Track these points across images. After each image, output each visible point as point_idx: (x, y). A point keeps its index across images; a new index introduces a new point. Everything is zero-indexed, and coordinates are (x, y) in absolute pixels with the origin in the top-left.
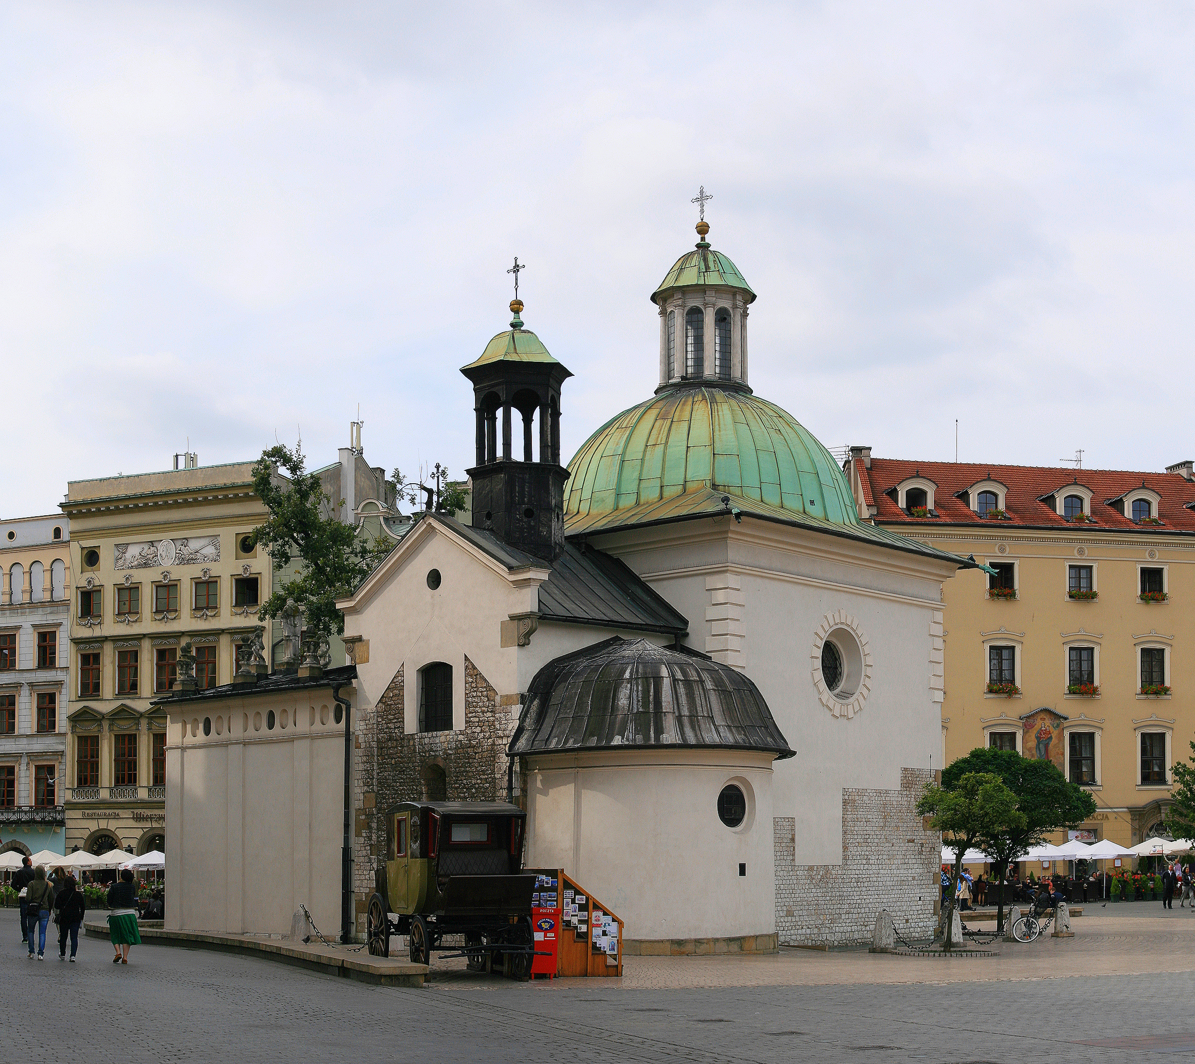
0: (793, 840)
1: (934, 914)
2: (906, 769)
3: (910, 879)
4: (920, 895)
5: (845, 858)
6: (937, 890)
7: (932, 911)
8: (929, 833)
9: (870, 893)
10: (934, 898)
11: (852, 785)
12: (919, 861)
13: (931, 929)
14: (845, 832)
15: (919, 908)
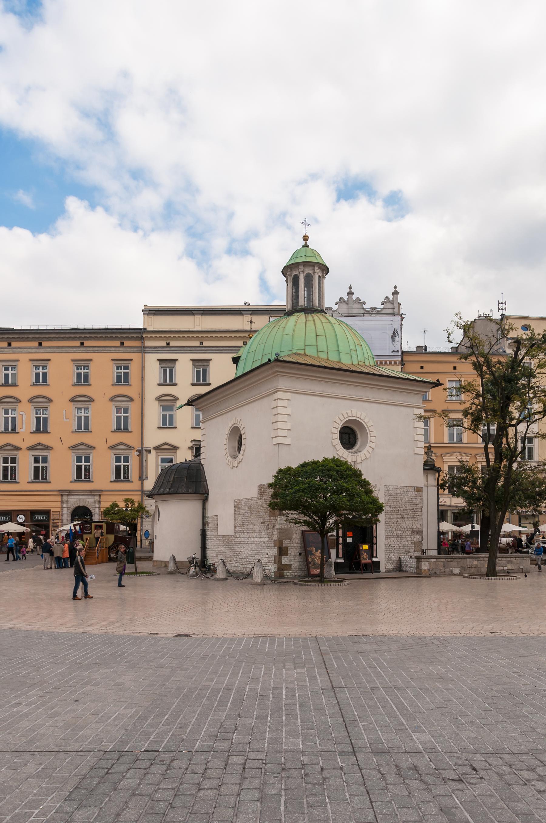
0: (217, 524)
1: (275, 563)
2: (260, 485)
3: (262, 543)
4: (267, 552)
5: (235, 533)
6: (276, 550)
7: (273, 562)
8: (272, 518)
9: (245, 549)
10: (274, 554)
11: (238, 498)
12: (266, 534)
13: (273, 571)
14: (235, 520)
15: (266, 559)
